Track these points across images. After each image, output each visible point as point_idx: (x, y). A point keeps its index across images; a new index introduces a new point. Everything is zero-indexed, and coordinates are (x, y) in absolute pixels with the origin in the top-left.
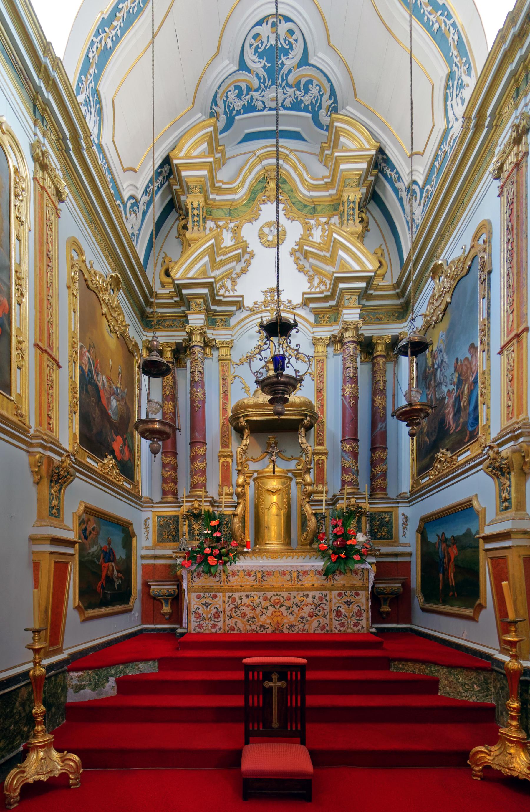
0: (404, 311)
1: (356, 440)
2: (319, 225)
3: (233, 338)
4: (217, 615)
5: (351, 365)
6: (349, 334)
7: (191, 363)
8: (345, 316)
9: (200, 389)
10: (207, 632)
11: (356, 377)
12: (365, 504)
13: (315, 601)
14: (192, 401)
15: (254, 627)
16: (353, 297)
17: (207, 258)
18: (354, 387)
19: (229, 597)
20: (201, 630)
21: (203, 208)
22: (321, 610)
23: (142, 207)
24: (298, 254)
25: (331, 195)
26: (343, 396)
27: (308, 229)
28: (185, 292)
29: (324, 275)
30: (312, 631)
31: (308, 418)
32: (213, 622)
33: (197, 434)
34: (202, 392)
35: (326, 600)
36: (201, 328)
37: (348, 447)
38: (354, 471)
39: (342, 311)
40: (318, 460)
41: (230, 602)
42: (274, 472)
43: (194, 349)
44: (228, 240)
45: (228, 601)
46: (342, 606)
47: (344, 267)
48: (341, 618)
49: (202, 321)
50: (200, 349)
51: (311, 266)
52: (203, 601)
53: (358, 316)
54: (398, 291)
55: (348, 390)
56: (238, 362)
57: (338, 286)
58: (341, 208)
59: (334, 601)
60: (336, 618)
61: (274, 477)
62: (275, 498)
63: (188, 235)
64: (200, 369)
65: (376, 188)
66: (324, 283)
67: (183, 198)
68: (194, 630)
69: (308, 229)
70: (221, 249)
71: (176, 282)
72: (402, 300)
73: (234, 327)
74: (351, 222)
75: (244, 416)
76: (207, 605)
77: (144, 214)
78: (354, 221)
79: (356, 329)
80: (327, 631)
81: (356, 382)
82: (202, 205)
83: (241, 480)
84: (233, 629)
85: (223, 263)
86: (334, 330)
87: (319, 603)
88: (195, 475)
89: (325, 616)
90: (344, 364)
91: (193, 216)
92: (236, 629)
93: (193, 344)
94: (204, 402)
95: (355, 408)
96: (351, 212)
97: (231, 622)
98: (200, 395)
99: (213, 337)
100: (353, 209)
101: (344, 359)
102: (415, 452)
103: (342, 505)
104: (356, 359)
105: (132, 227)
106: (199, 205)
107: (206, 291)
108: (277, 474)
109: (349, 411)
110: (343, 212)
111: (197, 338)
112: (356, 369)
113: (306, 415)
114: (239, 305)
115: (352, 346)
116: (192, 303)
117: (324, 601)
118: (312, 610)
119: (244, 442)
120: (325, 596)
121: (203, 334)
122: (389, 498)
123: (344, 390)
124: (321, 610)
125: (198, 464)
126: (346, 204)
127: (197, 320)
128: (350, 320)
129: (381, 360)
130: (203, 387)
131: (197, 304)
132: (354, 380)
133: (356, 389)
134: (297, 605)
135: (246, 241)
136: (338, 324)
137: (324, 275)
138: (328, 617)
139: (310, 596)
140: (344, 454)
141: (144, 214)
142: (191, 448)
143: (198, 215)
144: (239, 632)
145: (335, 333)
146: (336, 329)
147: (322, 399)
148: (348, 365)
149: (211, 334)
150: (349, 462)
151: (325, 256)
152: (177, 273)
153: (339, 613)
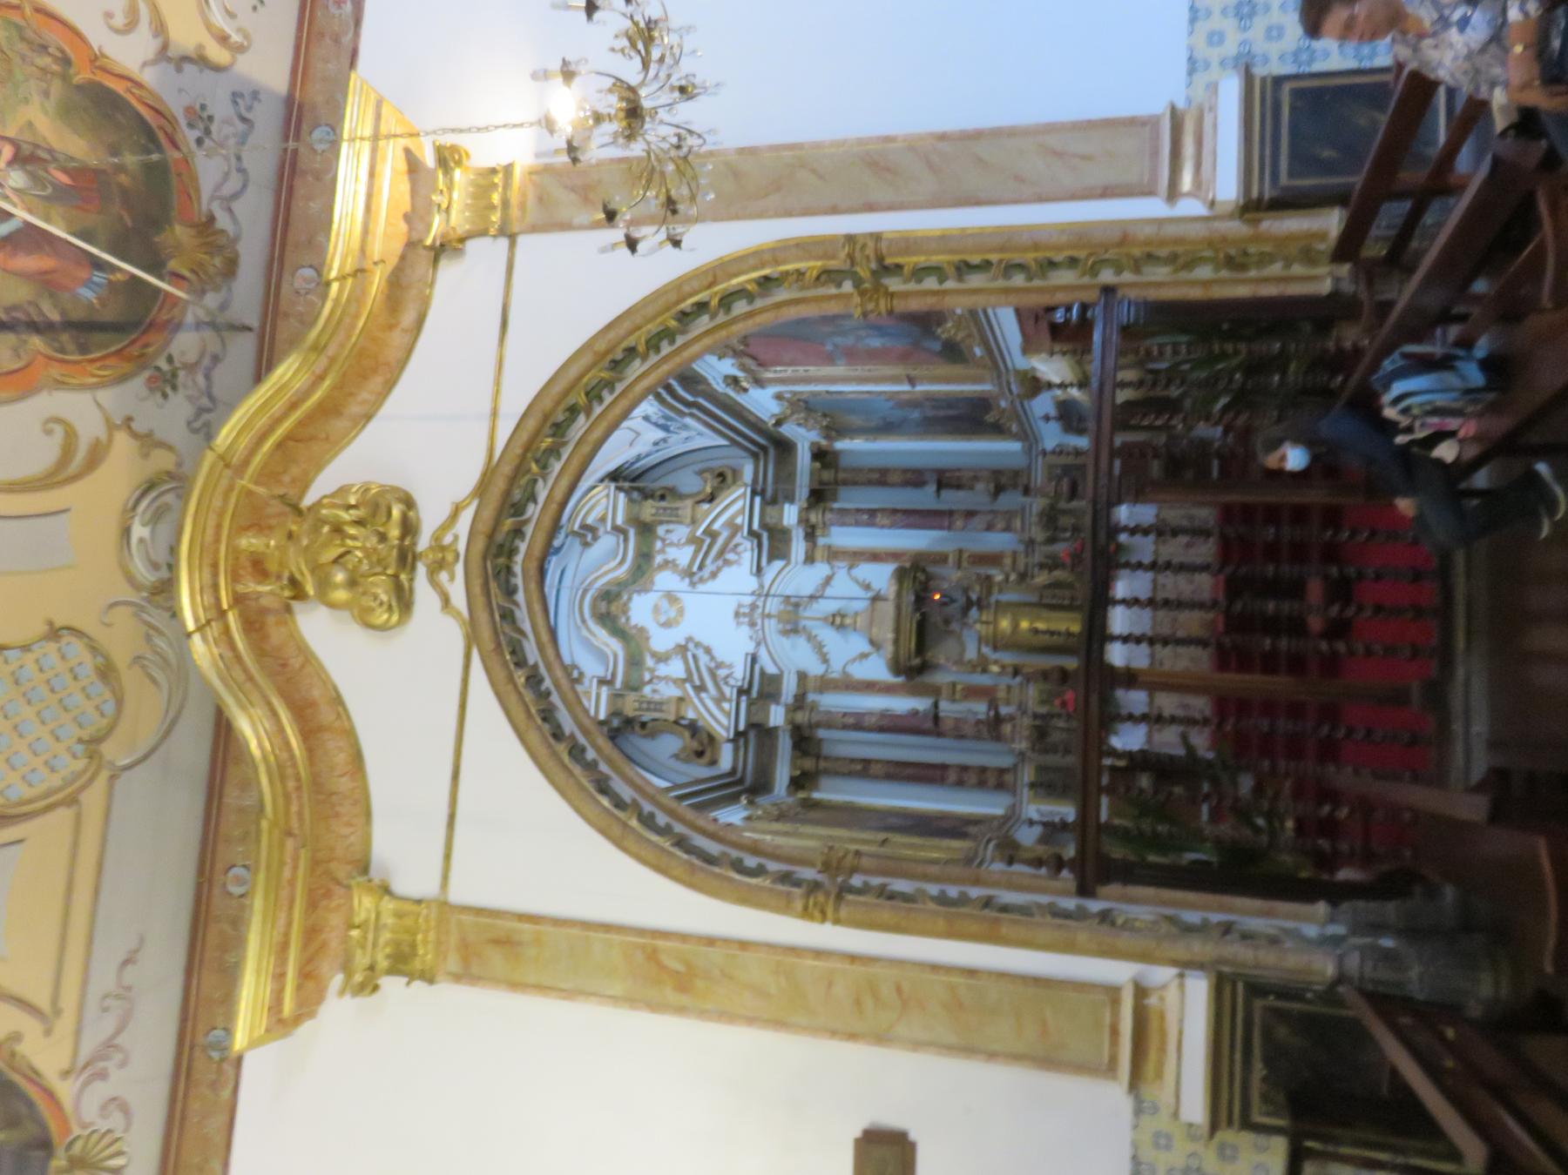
0: (784, 447)
12: (1038, 504)
17: (703, 695)
24: (696, 578)
27: (667, 564)
28: (742, 727)
37: (959, 523)
38: (989, 517)
42: (987, 623)
61: (995, 622)
62: (1024, 625)
69: (667, 564)
83: (995, 669)
98: (874, 720)
101: (843, 524)
103: (1039, 534)
108: (991, 618)
111: (801, 717)
116: (755, 719)
119: (942, 661)
122: (1029, 467)
123: (883, 527)
127: (776, 716)
132: (872, 513)
150: (978, 521)
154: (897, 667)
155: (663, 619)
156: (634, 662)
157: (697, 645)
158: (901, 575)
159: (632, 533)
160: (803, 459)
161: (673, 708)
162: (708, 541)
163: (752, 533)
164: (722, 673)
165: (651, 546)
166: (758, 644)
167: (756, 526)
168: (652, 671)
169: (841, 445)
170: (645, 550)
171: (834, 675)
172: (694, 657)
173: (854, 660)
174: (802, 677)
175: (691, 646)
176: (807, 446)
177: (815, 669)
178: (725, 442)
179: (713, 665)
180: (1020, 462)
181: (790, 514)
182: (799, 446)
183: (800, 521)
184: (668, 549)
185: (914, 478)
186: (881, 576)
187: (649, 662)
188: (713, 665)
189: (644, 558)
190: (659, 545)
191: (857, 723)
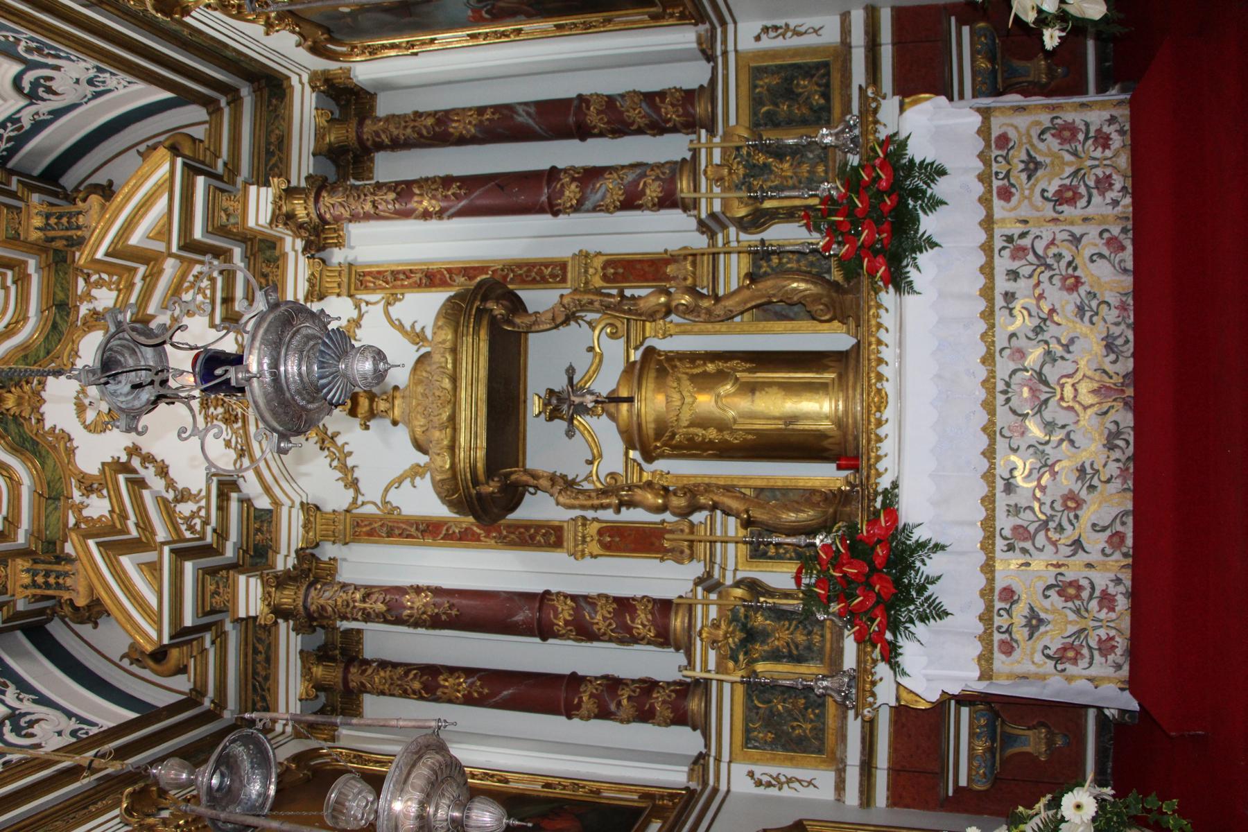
1: (553, 173)
2: (89, 294)
3: (297, 504)
4: (1067, 590)
5: (369, 198)
6: (301, 209)
7: (344, 617)
8: (262, 221)
9: (407, 600)
10: (1126, 624)
11: (398, 183)
13: (1026, 270)
14: (436, 623)
15: (1113, 469)
16: (225, 204)
17: (126, 561)
18: (420, 187)
19: (1011, 548)
20: (1121, 643)
21: (35, 562)
22: (1054, 250)
23: (26, 706)
25: (39, 268)
26: (440, 214)
29: (183, 278)
30: (1128, 281)
31: (490, 305)
32: (1094, 604)
33: (519, 617)
34: (413, 595)
35: (1023, 235)
36: (265, 584)
39: (251, 229)
40: (605, 278)
41: (1028, 545)
43: (313, 608)
44: (98, 507)
45: (1024, 551)
46: (1043, 184)
47: (163, 233)
48: (1082, 190)
49: (252, 580)
50: (313, 593)
51: (164, 307)
52: (1020, 634)
53: (263, 190)
54: (223, 103)
55: (425, 203)
56: (351, 492)
57: (199, 242)
58: (59, 244)
59: (1024, 212)
60: (1083, 202)
63: (81, 602)
64: (358, 596)
65: (36, 173)
66: (197, 277)
67: (21, 606)
68: (1118, 667)
70: (114, 526)
71: (166, 641)
72: (245, 91)
73: (276, 503)
74: (81, 220)
75: (476, 482)
76: (1035, 622)
77: (43, 701)
78: (80, 213)
79: (290, 192)
80: (1124, 230)
81: (409, 184)
82: (27, 565)
84: (1116, 540)
85: (145, 524)
86: (294, 249)
87: (1031, 257)
88: (629, 629)
89: (1076, 240)
90: (367, 217)
91: (47, 585)
92: (1118, 527)
93: (301, 609)
94: (438, 591)
95: (470, 182)
96: (64, 220)
97: (1096, 543)
99: (293, 555)
100: (60, 217)
101: (354, 218)
102: (593, 18)
104: (357, 187)
105: (60, 734)
106: (28, 571)
107: (189, 566)
109: (478, 197)
110: (68, 238)
111: (287, 598)
112: (379, 186)
113: (480, 312)
114: (227, 486)
115: (326, 199)
117: (1026, 242)
118: (1056, 280)
120: (1010, 239)
121: (283, 581)
123: (426, 215)
124: (1054, 250)
125: (599, 619)
126: (52, 234)
128: (270, 207)
129: (369, 128)
130: (401, 590)
131: (216, 593)
132: (404, 189)
133: (425, 183)
134: (1038, 330)
135: (103, 464)
136: (281, 239)
137: (183, 278)
138: (1077, 231)
139: (1010, 286)
140: (588, 204)
141: (43, 701)
142: (556, 636)
143: (47, 575)
144: (1130, 520)
145: (299, 244)
146: (292, 245)
147: (449, 270)
148: (368, 207)
149: (284, 561)
151: (144, 278)
152: (152, 634)
153: (1065, 197)
154: (458, 492)
155: (90, 416)
156: (52, 495)
157: (148, 459)
158: (454, 313)
159: (32, 264)
160: (305, 107)
161: (82, 588)
162: (142, 269)
163: (189, 245)
164: (185, 509)
165: (68, 288)
166: (241, 455)
167: (198, 234)
168: (79, 508)
169: (364, 71)
170: (61, 296)
171: (369, 509)
172: (138, 484)
173: (399, 481)
174: (311, 510)
175: (136, 462)
176: (305, 78)
177: (336, 498)
178: (167, 95)
179: (170, 496)
180: (694, 75)
181: (259, 207)
182: (295, 80)
183: (275, 219)
184: (94, 292)
185: (501, 125)
186: (423, 308)
187: (77, 495)
188: (170, 496)
189: (61, 308)
190: (81, 282)
191: (393, 607)
